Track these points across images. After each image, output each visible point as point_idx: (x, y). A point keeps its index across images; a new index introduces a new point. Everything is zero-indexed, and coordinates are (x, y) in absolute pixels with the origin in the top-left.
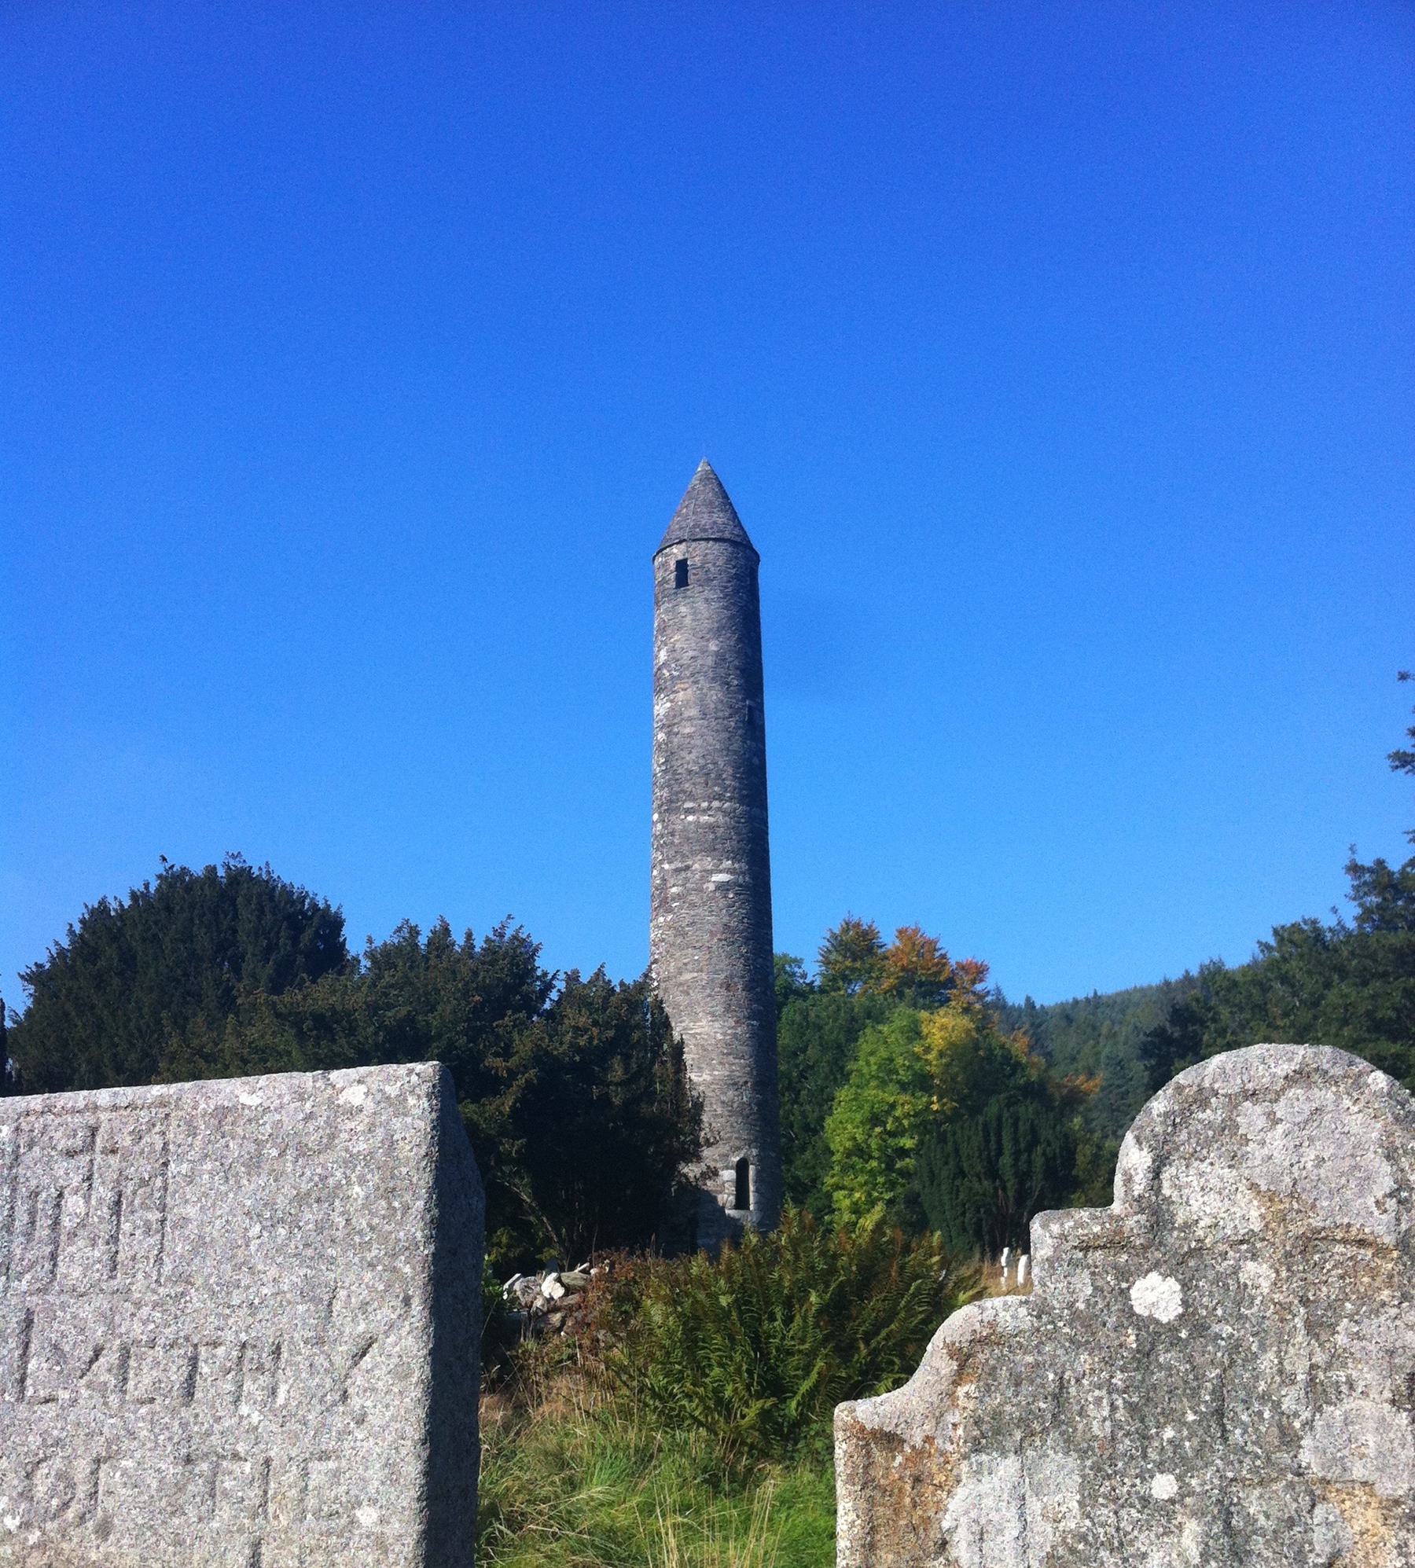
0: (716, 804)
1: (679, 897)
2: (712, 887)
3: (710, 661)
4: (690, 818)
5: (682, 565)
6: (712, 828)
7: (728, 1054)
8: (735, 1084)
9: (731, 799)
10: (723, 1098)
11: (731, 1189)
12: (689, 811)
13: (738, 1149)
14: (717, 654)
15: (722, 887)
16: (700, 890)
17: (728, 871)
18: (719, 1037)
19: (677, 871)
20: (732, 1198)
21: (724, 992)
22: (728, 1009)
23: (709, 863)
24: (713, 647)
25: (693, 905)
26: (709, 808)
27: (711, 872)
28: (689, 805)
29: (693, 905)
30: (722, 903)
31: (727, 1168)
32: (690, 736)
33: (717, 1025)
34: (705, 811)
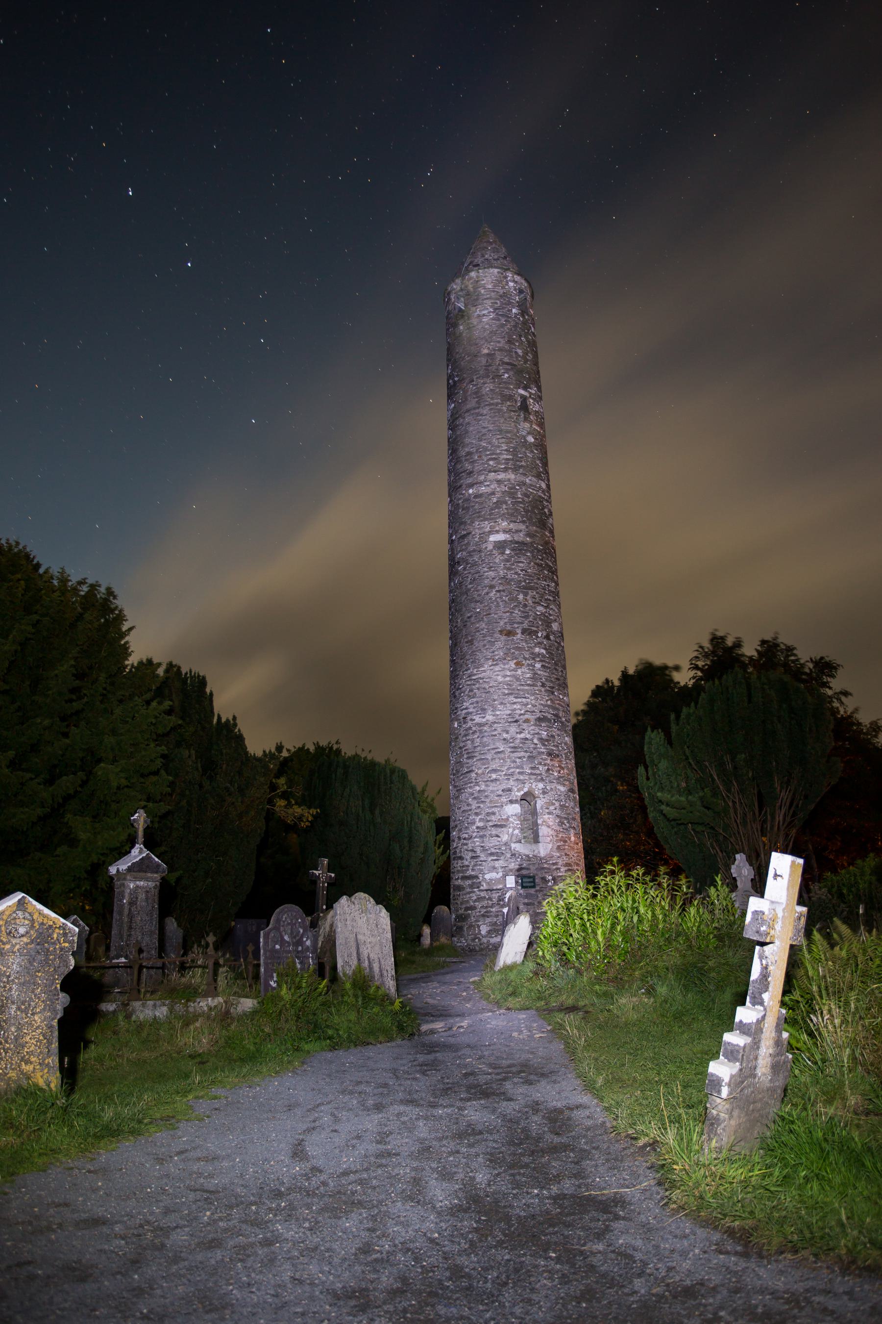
2: (490, 547)
3: (483, 361)
4: (471, 491)
7: (511, 694)
8: (516, 721)
9: (505, 470)
10: (505, 735)
12: (471, 486)
15: (500, 546)
17: (505, 532)
18: (500, 679)
19: (463, 537)
21: (503, 638)
23: (487, 526)
24: (486, 351)
25: (475, 564)
27: (491, 532)
28: (469, 480)
30: (498, 559)
31: (511, 802)
33: (497, 668)
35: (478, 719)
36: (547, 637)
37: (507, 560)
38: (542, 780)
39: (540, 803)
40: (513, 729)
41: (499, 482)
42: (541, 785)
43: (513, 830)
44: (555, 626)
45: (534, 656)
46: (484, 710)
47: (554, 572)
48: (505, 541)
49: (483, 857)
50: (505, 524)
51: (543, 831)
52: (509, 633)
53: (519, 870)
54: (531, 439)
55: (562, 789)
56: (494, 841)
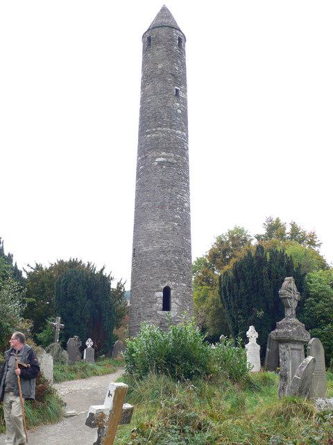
0: (159, 129)
1: (142, 170)
2: (156, 163)
5: (149, 39)
6: (157, 139)
8: (163, 252)
9: (166, 126)
11: (161, 301)
12: (148, 133)
13: (165, 282)
14: (162, 69)
15: (160, 164)
16: (150, 166)
20: (161, 306)
22: (161, 217)
23: (154, 154)
24: (160, 67)
25: (148, 172)
26: (156, 131)
27: (156, 157)
29: (148, 172)
31: (158, 291)
32: (149, 103)
33: (156, 225)
34: (154, 132)
35: (145, 249)
36: (181, 210)
37: (164, 172)
38: (175, 281)
39: (172, 292)
40: (162, 256)
41: (162, 132)
42: (174, 283)
43: (160, 304)
44: (186, 204)
45: (174, 220)
46: (148, 246)
47: (188, 178)
48: (163, 162)
49: (143, 317)
50: (164, 153)
51: (173, 305)
52: (163, 207)
53: (161, 324)
54: (179, 111)
55: (184, 285)
56: (148, 310)
